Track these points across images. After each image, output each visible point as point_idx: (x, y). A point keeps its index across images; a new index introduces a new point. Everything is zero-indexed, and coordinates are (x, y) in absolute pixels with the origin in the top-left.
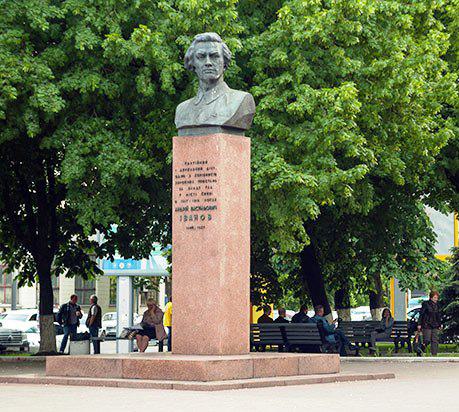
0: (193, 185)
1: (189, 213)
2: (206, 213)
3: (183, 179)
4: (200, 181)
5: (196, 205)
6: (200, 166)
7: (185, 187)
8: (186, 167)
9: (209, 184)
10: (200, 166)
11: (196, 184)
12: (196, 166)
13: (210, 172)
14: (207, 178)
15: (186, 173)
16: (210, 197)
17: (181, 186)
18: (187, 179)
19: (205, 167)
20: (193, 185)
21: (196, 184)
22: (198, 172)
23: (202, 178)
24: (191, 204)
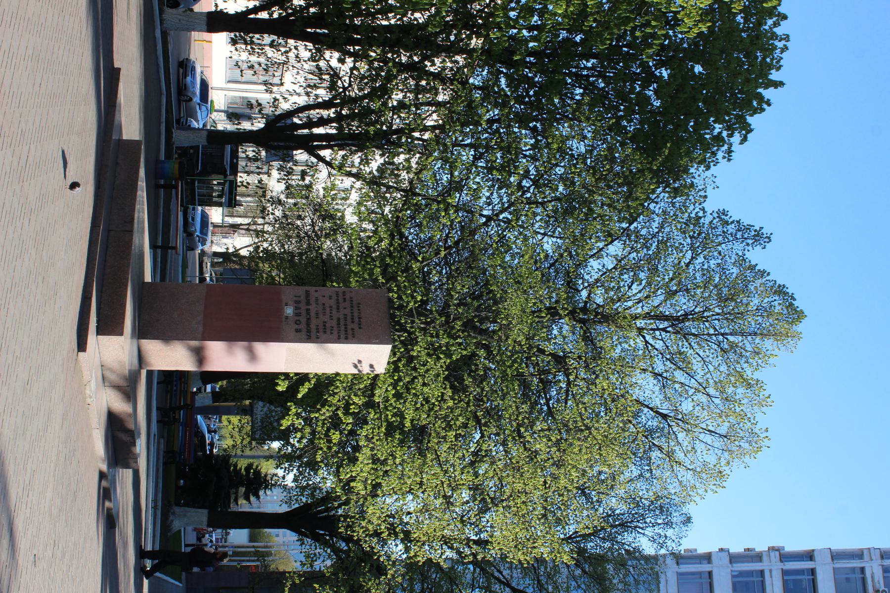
0: (334, 312)
1: (303, 306)
2: (303, 326)
3: (341, 300)
4: (339, 320)
5: (313, 314)
6: (356, 320)
7: (332, 302)
8: (354, 303)
9: (335, 329)
10: (356, 320)
11: (335, 315)
12: (356, 315)
13: (350, 332)
14: (343, 328)
15: (348, 304)
16: (321, 330)
17: (334, 297)
18: (342, 305)
19: (355, 326)
20: (334, 312)
21: (335, 315)
22: (349, 318)
23: (342, 322)
24: (313, 308)
